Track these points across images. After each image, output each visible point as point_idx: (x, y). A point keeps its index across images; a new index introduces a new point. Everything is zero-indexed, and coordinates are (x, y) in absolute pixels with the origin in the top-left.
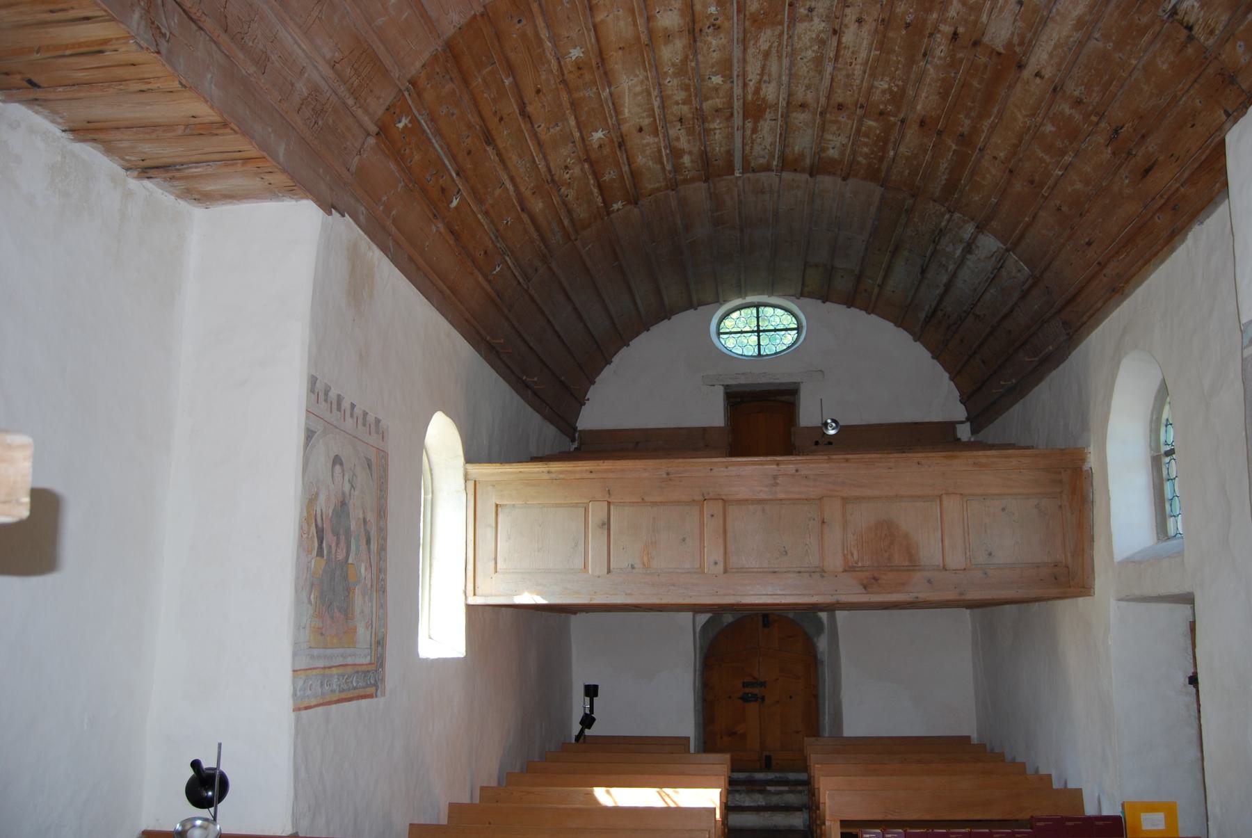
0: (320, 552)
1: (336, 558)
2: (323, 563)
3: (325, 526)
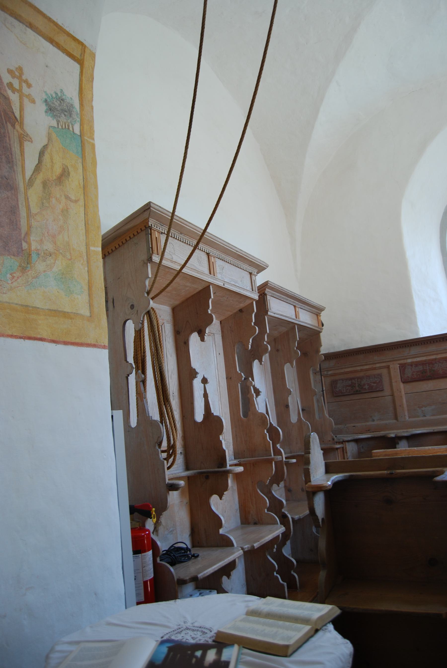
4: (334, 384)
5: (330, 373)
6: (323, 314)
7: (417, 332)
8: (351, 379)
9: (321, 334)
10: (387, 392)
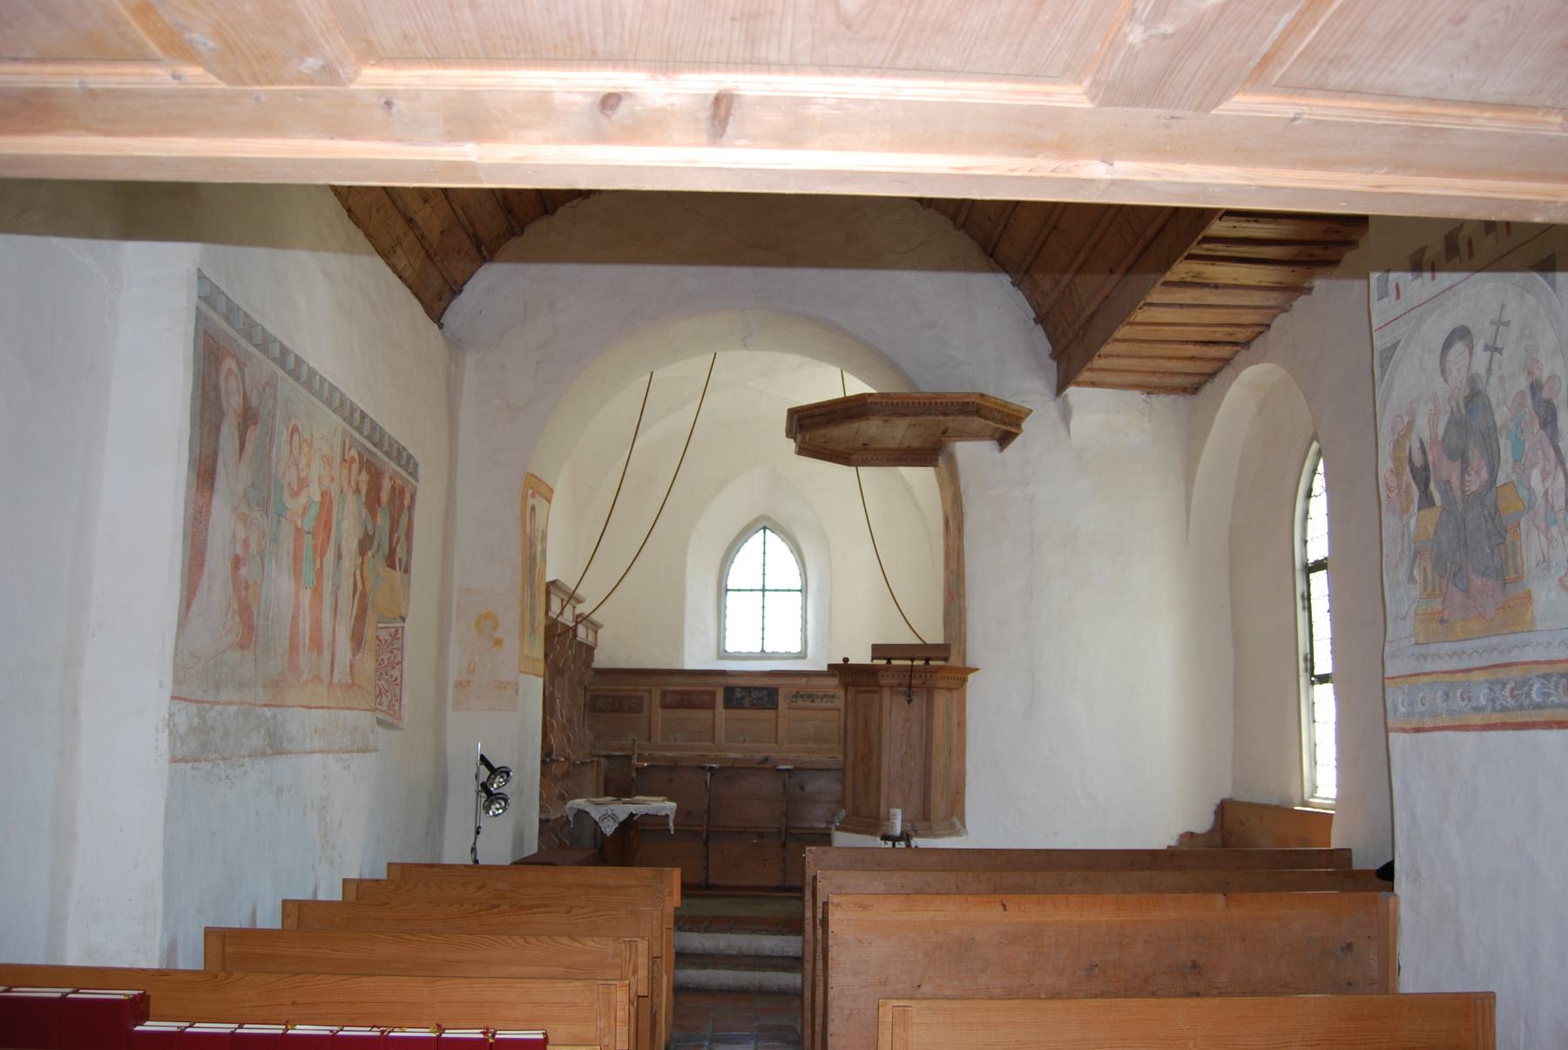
0: (1426, 500)
1: (1463, 492)
2: (1432, 515)
3: (1430, 458)
4: (595, 698)
5: (592, 687)
6: (600, 631)
9: (596, 652)
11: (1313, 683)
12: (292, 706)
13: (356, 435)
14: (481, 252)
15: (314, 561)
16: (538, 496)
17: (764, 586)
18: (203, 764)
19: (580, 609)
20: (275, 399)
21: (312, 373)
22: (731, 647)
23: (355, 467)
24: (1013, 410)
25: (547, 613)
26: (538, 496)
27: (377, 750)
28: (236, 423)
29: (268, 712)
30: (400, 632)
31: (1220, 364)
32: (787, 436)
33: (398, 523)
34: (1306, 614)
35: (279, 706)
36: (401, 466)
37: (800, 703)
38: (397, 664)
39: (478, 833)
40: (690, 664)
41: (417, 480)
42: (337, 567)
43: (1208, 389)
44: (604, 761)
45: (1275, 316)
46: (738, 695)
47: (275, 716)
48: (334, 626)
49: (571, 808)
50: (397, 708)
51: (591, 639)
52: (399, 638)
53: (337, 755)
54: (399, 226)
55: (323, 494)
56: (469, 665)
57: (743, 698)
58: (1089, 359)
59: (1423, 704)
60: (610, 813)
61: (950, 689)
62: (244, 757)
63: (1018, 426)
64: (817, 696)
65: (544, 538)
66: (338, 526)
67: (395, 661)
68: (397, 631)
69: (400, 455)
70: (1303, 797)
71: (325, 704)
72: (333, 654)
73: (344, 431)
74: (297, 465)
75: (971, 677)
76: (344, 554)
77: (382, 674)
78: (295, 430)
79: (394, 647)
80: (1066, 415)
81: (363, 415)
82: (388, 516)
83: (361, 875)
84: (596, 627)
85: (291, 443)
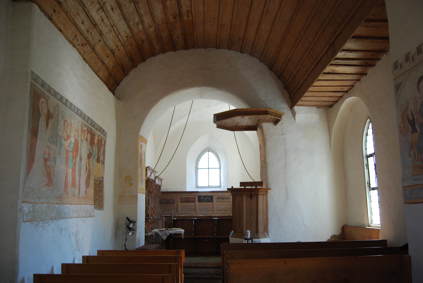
0: (414, 130)
3: (415, 117)
4: (161, 200)
5: (161, 197)
6: (162, 181)
7: (186, 190)
8: (166, 200)
9: (161, 187)
10: (176, 204)
11: (370, 190)
12: (66, 204)
13: (86, 123)
14: (125, 72)
15: (73, 160)
16: (142, 142)
17: (209, 167)
18: (34, 223)
19: (157, 175)
20: (59, 112)
21: (71, 104)
22: (200, 185)
23: (86, 133)
24: (279, 113)
25: (146, 176)
26: (142, 142)
27: (94, 216)
28: (45, 118)
29: (57, 206)
30: (102, 182)
31: (339, 98)
32: (214, 123)
33: (100, 150)
34: (367, 170)
35: (61, 204)
36: (101, 133)
37: (220, 200)
38: (101, 191)
39: (126, 240)
40: (188, 190)
41: (106, 137)
42: (80, 162)
43: (336, 106)
44: (164, 218)
45: (355, 83)
46: (202, 198)
47: (60, 207)
48: (80, 180)
49: (153, 232)
50: (101, 204)
51: (160, 184)
52: (101, 183)
53: (81, 218)
54: (100, 64)
55: (75, 141)
56: (123, 191)
57: (203, 199)
58: (301, 97)
59: (416, 195)
60: (165, 233)
61: (263, 195)
62: (49, 220)
63: (281, 118)
64: (224, 198)
65: (145, 154)
66: (81, 150)
67: (101, 190)
68: (101, 181)
69: (101, 130)
70: (368, 224)
71: (77, 203)
72: (79, 188)
73: (82, 122)
74: (66, 131)
75: (269, 191)
76: (83, 158)
77: (96, 194)
78: (66, 121)
79: (100, 186)
80: (294, 114)
81: (88, 118)
82: (97, 148)
83: (89, 255)
84: (161, 180)
85: (64, 124)
